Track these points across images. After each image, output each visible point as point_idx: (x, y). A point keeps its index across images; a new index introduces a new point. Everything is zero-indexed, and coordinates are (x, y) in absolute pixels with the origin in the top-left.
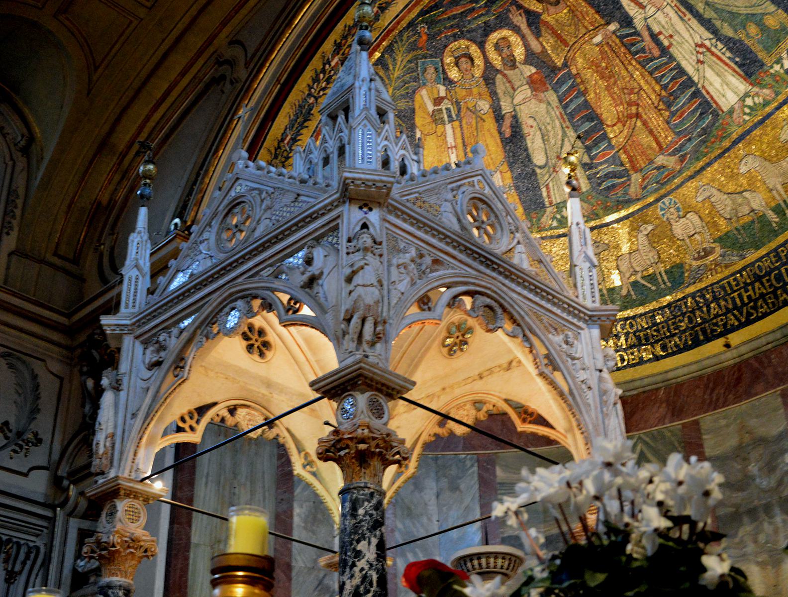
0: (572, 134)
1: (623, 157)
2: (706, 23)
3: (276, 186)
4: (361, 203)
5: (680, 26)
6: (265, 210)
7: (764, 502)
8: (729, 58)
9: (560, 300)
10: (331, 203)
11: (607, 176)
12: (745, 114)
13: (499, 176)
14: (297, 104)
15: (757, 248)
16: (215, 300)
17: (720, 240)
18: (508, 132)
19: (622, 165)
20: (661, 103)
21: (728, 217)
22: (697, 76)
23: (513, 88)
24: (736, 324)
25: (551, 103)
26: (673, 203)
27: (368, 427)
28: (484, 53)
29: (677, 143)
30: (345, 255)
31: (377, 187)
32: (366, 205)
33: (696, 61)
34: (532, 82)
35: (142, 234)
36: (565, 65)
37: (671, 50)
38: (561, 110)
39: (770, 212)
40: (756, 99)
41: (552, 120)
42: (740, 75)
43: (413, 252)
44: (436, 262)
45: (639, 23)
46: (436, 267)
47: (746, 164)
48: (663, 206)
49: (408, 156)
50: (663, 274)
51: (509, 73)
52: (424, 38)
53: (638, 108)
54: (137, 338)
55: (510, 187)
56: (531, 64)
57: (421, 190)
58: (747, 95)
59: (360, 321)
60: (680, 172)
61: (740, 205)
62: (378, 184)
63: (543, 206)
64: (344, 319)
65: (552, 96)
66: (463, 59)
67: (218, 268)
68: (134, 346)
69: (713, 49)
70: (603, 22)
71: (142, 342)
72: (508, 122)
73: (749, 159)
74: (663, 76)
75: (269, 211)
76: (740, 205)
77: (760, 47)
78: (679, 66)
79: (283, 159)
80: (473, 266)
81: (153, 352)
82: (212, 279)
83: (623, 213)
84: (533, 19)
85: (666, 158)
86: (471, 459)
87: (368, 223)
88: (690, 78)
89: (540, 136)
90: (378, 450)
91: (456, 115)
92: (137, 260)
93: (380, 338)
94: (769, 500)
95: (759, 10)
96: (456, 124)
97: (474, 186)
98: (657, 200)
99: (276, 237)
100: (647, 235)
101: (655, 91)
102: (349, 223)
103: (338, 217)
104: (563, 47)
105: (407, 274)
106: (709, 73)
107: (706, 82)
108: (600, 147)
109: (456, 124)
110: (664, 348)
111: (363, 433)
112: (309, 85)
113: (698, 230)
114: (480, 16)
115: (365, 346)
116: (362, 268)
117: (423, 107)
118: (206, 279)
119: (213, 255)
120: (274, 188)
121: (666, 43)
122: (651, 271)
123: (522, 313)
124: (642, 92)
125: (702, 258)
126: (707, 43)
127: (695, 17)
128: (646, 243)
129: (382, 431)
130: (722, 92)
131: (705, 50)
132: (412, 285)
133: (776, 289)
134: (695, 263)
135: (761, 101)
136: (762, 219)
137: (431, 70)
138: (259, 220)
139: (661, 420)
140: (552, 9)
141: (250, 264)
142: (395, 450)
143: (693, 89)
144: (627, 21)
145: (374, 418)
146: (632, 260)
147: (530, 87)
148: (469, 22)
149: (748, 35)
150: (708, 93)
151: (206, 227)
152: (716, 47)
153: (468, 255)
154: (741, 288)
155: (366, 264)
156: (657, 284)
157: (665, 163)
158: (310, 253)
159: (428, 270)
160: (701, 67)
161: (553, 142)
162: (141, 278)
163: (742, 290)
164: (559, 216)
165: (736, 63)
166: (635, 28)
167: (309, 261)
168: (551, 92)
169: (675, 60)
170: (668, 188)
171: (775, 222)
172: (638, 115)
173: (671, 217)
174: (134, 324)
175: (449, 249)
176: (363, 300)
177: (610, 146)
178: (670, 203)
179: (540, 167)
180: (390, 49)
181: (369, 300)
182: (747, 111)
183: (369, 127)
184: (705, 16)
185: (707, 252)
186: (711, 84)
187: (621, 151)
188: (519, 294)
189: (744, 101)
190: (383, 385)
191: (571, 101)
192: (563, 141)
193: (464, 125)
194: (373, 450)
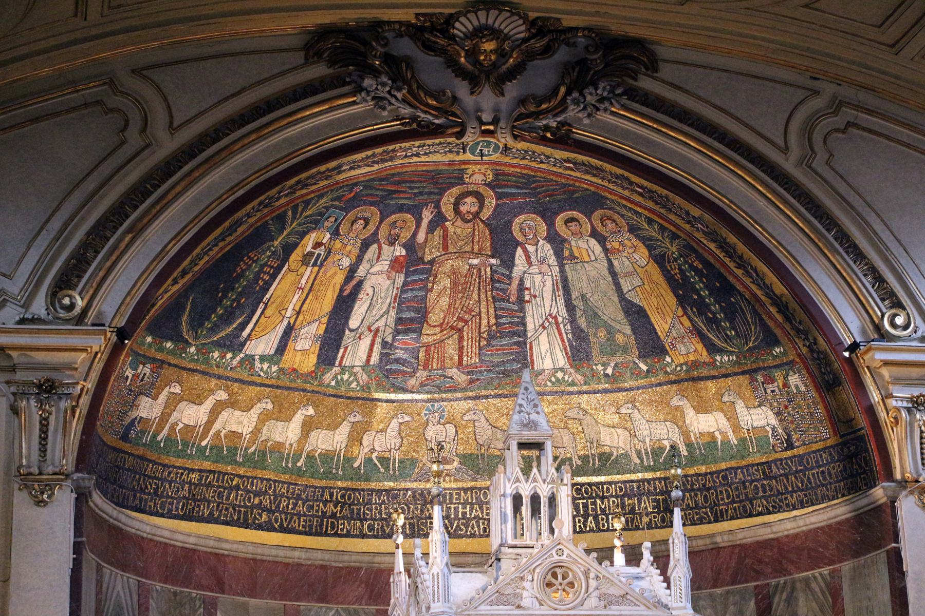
0: (393, 313)
1: (422, 355)
2: (570, 307)
5: (548, 295)
8: (569, 340)
11: (397, 361)
12: (550, 381)
19: (417, 358)
22: (532, 334)
23: (378, 259)
25: (396, 283)
28: (381, 222)
29: (477, 367)
36: (432, 262)
42: (566, 353)
52: (352, 195)
56: (404, 247)
58: (562, 369)
60: (463, 390)
61: (497, 439)
63: (334, 365)
65: (400, 279)
66: (361, 221)
69: (561, 326)
70: (489, 253)
72: (354, 282)
74: (503, 317)
76: (497, 439)
77: (597, 346)
83: (392, 396)
84: (438, 220)
86: (200, 599)
88: (525, 331)
89: (368, 305)
95: (618, 327)
96: (316, 269)
98: (428, 401)
101: (488, 323)
104: (441, 250)
106: (543, 338)
109: (316, 269)
110: (371, 528)
114: (402, 198)
117: (306, 245)
121: (527, 298)
122: (387, 455)
124: (478, 317)
126: (560, 319)
127: (564, 295)
128: (396, 429)
135: (570, 380)
137: (332, 219)
139: (358, 600)
140: (459, 222)
143: (521, 339)
144: (509, 263)
148: (392, 199)
149: (595, 335)
150: (531, 349)
152: (564, 326)
154: (458, 504)
156: (387, 469)
163: (460, 506)
164: (339, 377)
165: (571, 346)
166: (511, 272)
169: (524, 313)
170: (444, 396)
172: (460, 331)
173: (432, 419)
177: (417, 340)
178: (438, 409)
179: (351, 330)
180: (321, 196)
182: (553, 379)
184: (574, 302)
187: (424, 348)
191: (412, 290)
192: (382, 316)
193: (321, 274)
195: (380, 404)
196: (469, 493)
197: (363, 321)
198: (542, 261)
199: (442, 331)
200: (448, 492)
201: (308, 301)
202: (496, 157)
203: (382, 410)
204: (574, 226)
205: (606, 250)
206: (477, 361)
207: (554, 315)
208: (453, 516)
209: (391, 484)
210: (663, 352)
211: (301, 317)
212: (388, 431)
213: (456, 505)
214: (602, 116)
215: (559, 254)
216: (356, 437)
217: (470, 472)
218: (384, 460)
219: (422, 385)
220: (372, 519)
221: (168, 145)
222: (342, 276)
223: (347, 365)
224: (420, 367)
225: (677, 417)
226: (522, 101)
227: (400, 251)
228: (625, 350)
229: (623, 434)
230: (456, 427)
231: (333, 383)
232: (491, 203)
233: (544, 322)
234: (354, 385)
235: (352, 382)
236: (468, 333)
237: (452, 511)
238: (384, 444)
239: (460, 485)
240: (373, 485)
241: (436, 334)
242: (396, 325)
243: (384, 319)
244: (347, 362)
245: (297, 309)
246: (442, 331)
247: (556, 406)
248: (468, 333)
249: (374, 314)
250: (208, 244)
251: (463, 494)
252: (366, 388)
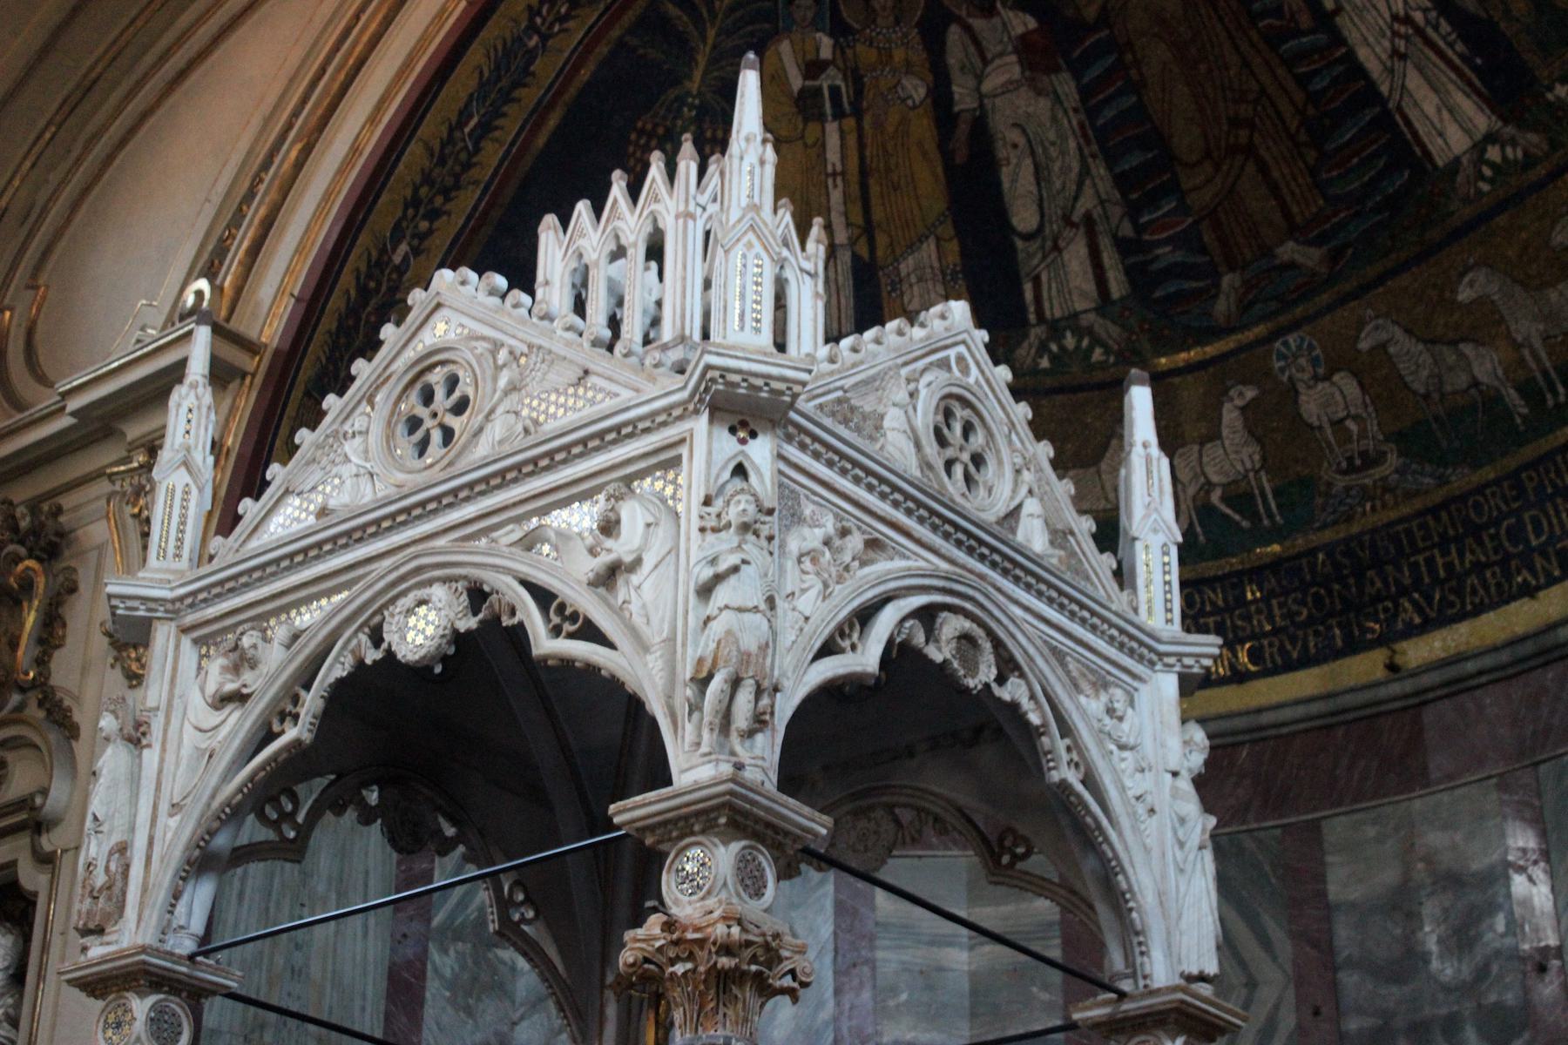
0: (1100, 170)
1: (1208, 238)
3: (536, 341)
4: (735, 420)
6: (506, 393)
7: (1444, 1011)
8: (1461, 56)
9: (1104, 620)
10: (668, 410)
11: (1171, 272)
12: (1482, 178)
13: (933, 247)
14: (500, 47)
15: (1476, 466)
16: (382, 577)
17: (1400, 438)
18: (961, 157)
19: (1203, 250)
20: (1303, 131)
21: (1422, 391)
24: (1417, 620)
25: (1063, 97)
26: (1305, 346)
27: (740, 922)
30: (695, 533)
31: (772, 391)
32: (744, 424)
33: (1389, 51)
34: (1025, 47)
35: (200, 390)
36: (1104, 18)
37: (1338, 20)
38: (1083, 117)
39: (1512, 391)
40: (1509, 150)
41: (1063, 138)
42: (1479, 94)
43: (829, 525)
44: (873, 544)
46: (871, 554)
47: (1471, 284)
48: (1283, 350)
49: (792, 259)
50: (1270, 496)
51: (978, 23)
53: (1251, 136)
54: (185, 630)
55: (954, 273)
56: (1024, 9)
57: (848, 383)
58: (1491, 138)
59: (727, 688)
61: (1451, 369)
62: (776, 385)
63: (1025, 323)
64: (692, 679)
65: (1066, 85)
67: (392, 508)
68: (177, 647)
69: (1430, 31)
71: (196, 642)
72: (963, 130)
73: (1481, 276)
74: (1316, 72)
75: (515, 397)
76: (1451, 369)
78: (1351, 56)
79: (458, 169)
80: (943, 551)
81: (225, 669)
82: (376, 528)
83: (1193, 354)
85: (1300, 248)
87: (746, 464)
88: (1371, 86)
89: (1031, 168)
90: (754, 968)
91: (850, 103)
92: (188, 450)
93: (764, 723)
94: (1455, 1008)
97: (949, 369)
99: (534, 461)
100: (1243, 409)
101: (1292, 101)
102: (709, 463)
103: (682, 441)
105: (818, 574)
106: (1414, 81)
107: (1406, 98)
108: (1159, 208)
109: (850, 123)
110: (1254, 656)
111: (729, 934)
112: (530, 7)
113: (1353, 411)
115: (735, 739)
116: (735, 569)
118: (364, 527)
119: (376, 470)
120: (530, 346)
123: (1032, 650)
125: (1358, 470)
126: (1418, 16)
128: (1239, 424)
129: (765, 928)
130: (1438, 126)
131: (1410, 31)
132: (824, 598)
133: (1507, 557)
134: (1341, 482)
135: (1520, 154)
138: (492, 411)
141: (469, 510)
142: (786, 965)
143: (1377, 110)
145: (746, 897)
146: (1205, 459)
147: (1020, 62)
150: (1408, 123)
151: (359, 402)
152: (1436, 28)
153: (935, 528)
154: (1433, 546)
155: (744, 562)
156: (1254, 517)
157: (1299, 258)
158: (612, 509)
159: (856, 563)
160: (1398, 65)
161: (1058, 184)
162: (194, 491)
163: (1436, 552)
164: (1054, 347)
165: (1475, 69)
167: (609, 527)
168: (1066, 75)
170: (1299, 311)
171: (1519, 414)
172: (1250, 151)
173: (1299, 375)
174: (181, 599)
175: (900, 516)
176: (737, 642)
178: (1299, 347)
179: (1028, 237)
181: (750, 643)
182: (1487, 172)
183: (758, 248)
185: (1370, 460)
186: (1416, 104)
188: (1027, 609)
189: (1484, 151)
190: (768, 825)
191: (1107, 101)
192: (1080, 184)
194: (745, 967)
195: (1177, 380)
196: (1444, 515)
197: (1041, 207)
199: (1217, 167)
200: (1400, 528)
201: (875, 201)
206: (1321, 202)
207: (1402, 13)
208: (1427, 580)
209: (1276, 548)
211: (881, 240)
212: (1225, 432)
213: (1428, 554)
217: (1428, 468)
218: (1240, 497)
219: (1245, 307)
220: (1253, 637)
222: (925, 122)
223: (1058, 314)
224: (1220, 269)
230: (1355, 375)
231: (1045, 363)
233: (1392, 43)
234: (1098, 355)
235: (1090, 349)
236: (1268, 148)
237: (1423, 569)
238: (1227, 467)
239: (1418, 504)
240: (1235, 563)
241: (1208, 181)
242: (1124, 195)
243: (1088, 191)
244: (1054, 310)
245: (860, 220)
246: (1217, 167)
247: (1524, 235)
248: (1268, 148)
249: (1058, 184)
250: (464, 115)
251: (1432, 523)
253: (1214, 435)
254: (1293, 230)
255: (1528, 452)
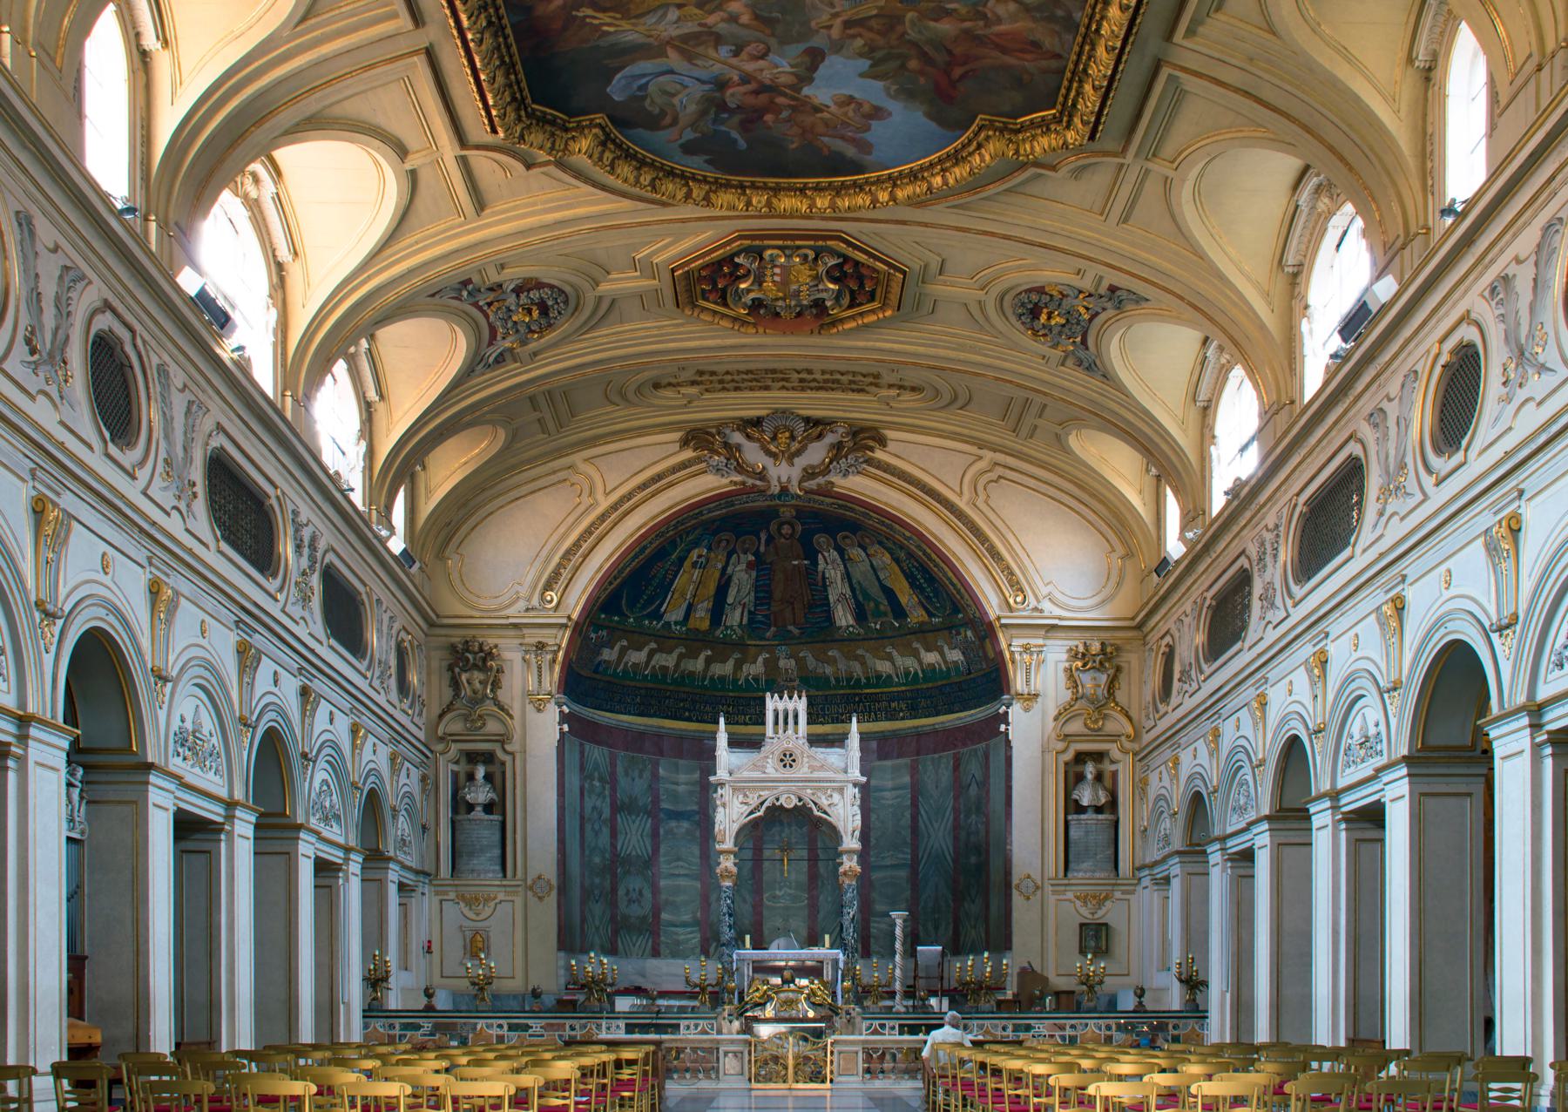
0: (753, 594)
5: (839, 581)
18: (723, 582)
36: (771, 563)
45: (820, 568)
65: (754, 574)
88: (829, 604)
106: (839, 607)
136: (827, 679)
144: (815, 563)
172: (792, 604)
180: (695, 529)
185: (791, 680)
198: (833, 561)
202: (793, 502)
203: (752, 650)
204: (848, 541)
205: (868, 555)
210: (907, 616)
214: (851, 477)
215: (842, 556)
216: (738, 666)
218: (756, 679)
221: (604, 504)
225: (916, 654)
226: (805, 470)
227: (751, 558)
228: (885, 614)
229: (888, 664)
232: (799, 528)
244: (728, 624)
252: (741, 638)
253: (755, 662)
254: (794, 624)
255: (832, 692)
